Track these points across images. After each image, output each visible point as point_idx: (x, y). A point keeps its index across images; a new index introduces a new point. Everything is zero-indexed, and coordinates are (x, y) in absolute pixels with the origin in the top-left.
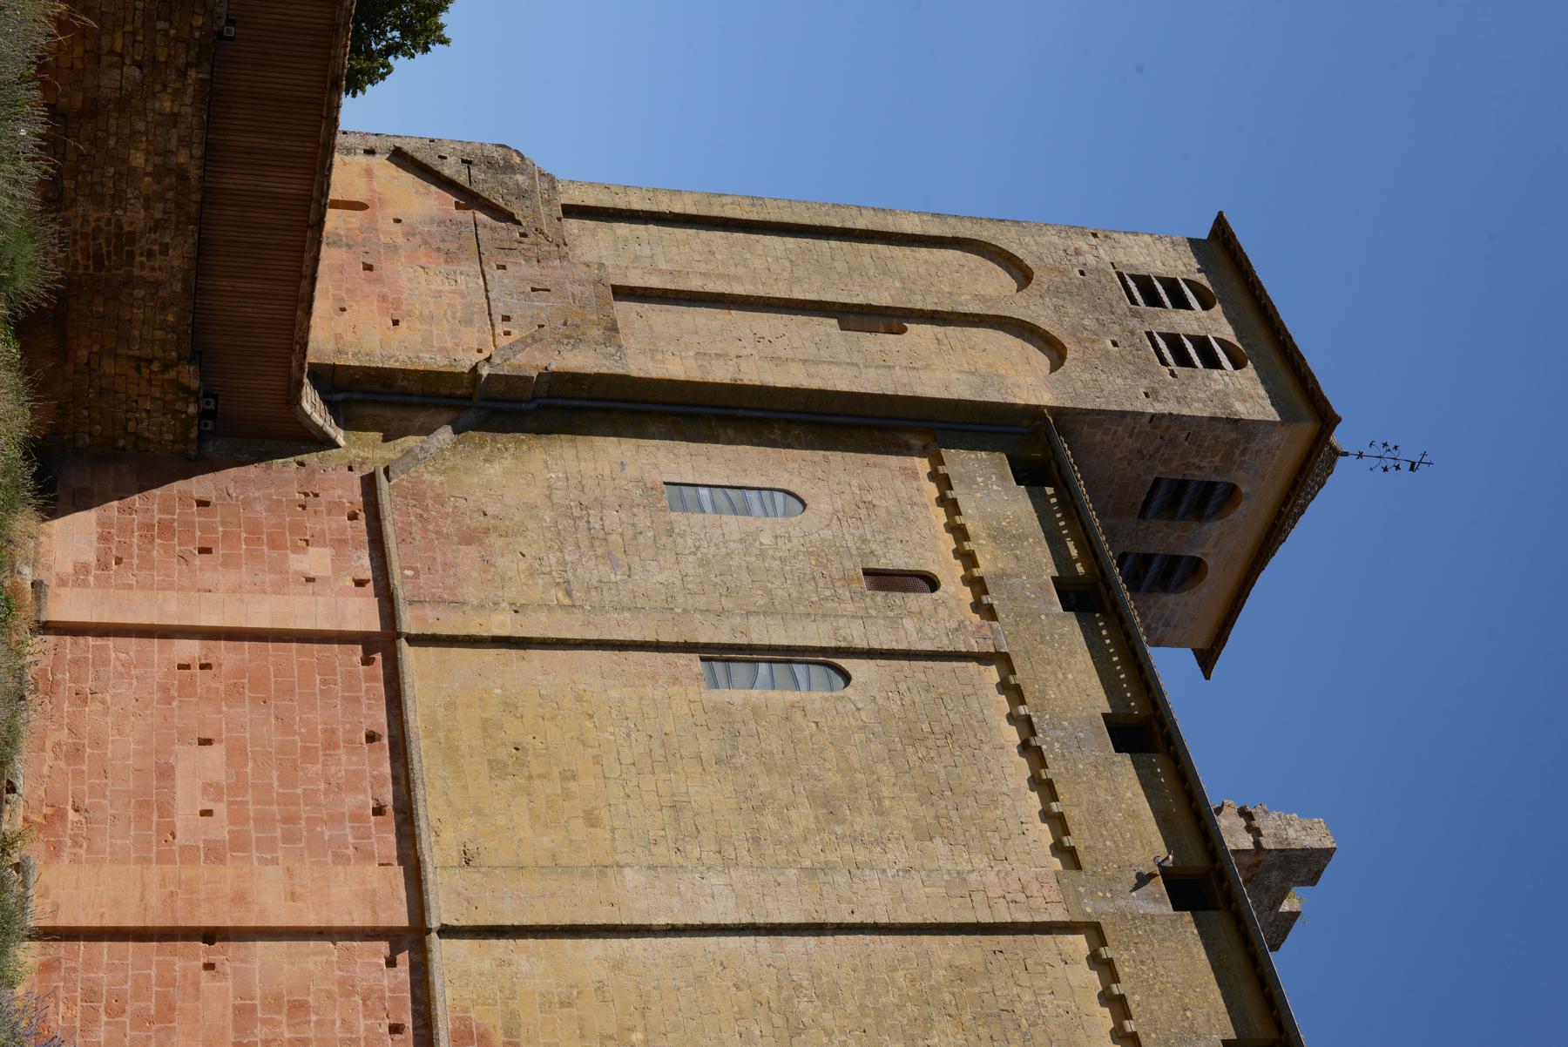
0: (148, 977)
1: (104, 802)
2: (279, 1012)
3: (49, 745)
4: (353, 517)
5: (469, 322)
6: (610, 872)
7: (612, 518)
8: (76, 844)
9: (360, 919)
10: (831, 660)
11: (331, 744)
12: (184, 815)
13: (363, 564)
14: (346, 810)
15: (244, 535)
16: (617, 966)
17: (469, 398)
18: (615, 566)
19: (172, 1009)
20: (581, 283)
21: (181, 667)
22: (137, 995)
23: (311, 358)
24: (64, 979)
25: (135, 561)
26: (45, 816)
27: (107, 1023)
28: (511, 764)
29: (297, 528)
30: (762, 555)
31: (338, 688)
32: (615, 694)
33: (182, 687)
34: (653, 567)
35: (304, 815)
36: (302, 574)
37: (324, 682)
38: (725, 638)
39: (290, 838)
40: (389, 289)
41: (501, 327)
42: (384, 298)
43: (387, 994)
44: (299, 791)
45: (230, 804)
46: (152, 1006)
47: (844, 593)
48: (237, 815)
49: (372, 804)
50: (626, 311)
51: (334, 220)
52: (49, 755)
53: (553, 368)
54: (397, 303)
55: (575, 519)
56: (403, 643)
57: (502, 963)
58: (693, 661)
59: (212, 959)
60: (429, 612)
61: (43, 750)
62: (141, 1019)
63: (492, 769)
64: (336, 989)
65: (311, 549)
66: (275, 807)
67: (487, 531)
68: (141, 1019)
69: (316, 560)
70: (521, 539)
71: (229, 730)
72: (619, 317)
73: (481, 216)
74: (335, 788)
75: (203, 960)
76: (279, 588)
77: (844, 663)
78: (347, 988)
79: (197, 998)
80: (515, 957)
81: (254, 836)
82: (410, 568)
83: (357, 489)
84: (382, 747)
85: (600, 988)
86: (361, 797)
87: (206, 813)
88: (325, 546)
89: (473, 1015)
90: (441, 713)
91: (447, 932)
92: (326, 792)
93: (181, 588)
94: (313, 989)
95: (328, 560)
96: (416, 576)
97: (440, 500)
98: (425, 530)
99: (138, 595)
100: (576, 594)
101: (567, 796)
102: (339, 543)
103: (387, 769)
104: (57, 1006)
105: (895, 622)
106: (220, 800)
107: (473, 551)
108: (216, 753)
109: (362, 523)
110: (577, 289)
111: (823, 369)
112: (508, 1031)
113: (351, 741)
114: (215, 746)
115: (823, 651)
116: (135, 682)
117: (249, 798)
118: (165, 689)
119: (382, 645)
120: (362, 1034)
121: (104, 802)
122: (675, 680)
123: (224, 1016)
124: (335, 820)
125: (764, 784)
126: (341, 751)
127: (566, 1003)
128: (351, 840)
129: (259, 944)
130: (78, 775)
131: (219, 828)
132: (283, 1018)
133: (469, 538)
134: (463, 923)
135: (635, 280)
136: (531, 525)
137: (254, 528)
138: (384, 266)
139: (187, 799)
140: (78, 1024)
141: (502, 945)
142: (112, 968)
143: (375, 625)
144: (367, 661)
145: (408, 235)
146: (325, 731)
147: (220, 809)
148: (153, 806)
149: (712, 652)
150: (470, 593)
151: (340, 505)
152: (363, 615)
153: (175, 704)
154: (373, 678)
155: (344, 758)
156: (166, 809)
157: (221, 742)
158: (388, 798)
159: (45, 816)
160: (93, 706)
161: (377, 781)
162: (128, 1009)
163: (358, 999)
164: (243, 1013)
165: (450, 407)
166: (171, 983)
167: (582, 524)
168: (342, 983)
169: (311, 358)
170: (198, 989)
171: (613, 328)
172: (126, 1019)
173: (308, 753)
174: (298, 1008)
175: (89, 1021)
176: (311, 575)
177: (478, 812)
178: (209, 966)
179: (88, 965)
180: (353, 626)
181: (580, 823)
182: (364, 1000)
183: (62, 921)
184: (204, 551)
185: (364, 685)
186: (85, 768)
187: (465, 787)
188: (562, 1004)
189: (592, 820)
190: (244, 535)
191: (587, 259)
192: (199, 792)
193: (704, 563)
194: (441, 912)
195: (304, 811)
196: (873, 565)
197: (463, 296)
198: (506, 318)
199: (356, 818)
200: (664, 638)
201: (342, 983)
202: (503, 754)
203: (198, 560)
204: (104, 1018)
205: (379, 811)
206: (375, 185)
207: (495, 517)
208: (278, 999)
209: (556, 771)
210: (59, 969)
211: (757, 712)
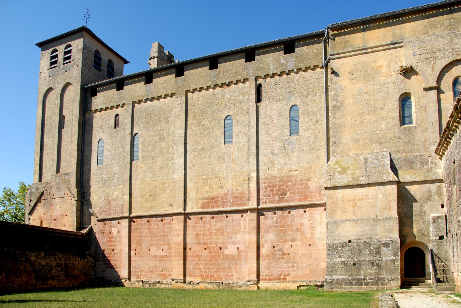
4: (106, 224)
5: (66, 202)
6: (174, 180)
7: (105, 176)
9: (182, 224)
10: (133, 136)
11: (150, 229)
12: (163, 253)
13: (115, 222)
16: (191, 180)
17: (81, 202)
18: (114, 176)
20: (56, 179)
22: (195, 261)
23: (75, 231)
28: (153, 197)
29: (108, 234)
30: (111, 148)
32: (140, 178)
33: (139, 254)
34: (114, 169)
38: (129, 156)
39: (167, 236)
40: (60, 215)
41: (66, 195)
42: (61, 217)
47: (119, 133)
48: (163, 245)
50: (62, 171)
51: (44, 225)
53: (75, 186)
54: (62, 215)
56: (131, 216)
57: (190, 200)
58: (134, 162)
60: (124, 211)
67: (108, 200)
69: (114, 231)
72: (63, 173)
73: (43, 198)
74: (158, 228)
76: (120, 237)
77: (134, 134)
78: (194, 226)
83: (100, 223)
85: (195, 183)
87: (163, 250)
90: (144, 209)
91: (185, 209)
93: (121, 254)
97: (102, 208)
98: (108, 211)
99: (123, 262)
100: (120, 184)
101: (159, 187)
102: (111, 227)
103: (154, 219)
105: (126, 124)
107: (112, 202)
109: (107, 222)
110: (57, 180)
111: (73, 133)
112: (202, 199)
113: (149, 225)
115: (131, 138)
117: (160, 243)
118: (140, 257)
119: (131, 219)
122: (137, 166)
124: (164, 228)
125: (157, 151)
127: (198, 189)
129: (187, 241)
131: (166, 248)
133: (109, 203)
134: (183, 206)
135: (55, 168)
136: (106, 191)
137: (109, 242)
138: (55, 218)
139: (160, 253)
141: (188, 200)
142: (190, 265)
143: (127, 220)
144: (134, 222)
145: (47, 212)
147: (162, 248)
149: (132, 159)
150: (120, 203)
151: (103, 226)
152: (125, 223)
154: (137, 221)
158: (160, 219)
161: (157, 221)
165: (83, 206)
167: (106, 182)
168: (193, 227)
169: (75, 231)
171: (66, 174)
173: (151, 233)
174: (198, 235)
177: (162, 203)
179: (190, 269)
180: (127, 224)
181: (165, 185)
183: (182, 273)
184: (113, 250)
188: (198, 190)
189: (164, 183)
191: (50, 178)
193: (113, 159)
194: (181, 210)
195: (162, 233)
196: (114, 126)
197: (60, 202)
198: (65, 194)
199: (163, 224)
200: (129, 168)
201: (193, 227)
202: (151, 198)
203: (115, 251)
205: (162, 220)
206: (37, 218)
208: (196, 238)
209: (155, 189)
211: (143, 151)
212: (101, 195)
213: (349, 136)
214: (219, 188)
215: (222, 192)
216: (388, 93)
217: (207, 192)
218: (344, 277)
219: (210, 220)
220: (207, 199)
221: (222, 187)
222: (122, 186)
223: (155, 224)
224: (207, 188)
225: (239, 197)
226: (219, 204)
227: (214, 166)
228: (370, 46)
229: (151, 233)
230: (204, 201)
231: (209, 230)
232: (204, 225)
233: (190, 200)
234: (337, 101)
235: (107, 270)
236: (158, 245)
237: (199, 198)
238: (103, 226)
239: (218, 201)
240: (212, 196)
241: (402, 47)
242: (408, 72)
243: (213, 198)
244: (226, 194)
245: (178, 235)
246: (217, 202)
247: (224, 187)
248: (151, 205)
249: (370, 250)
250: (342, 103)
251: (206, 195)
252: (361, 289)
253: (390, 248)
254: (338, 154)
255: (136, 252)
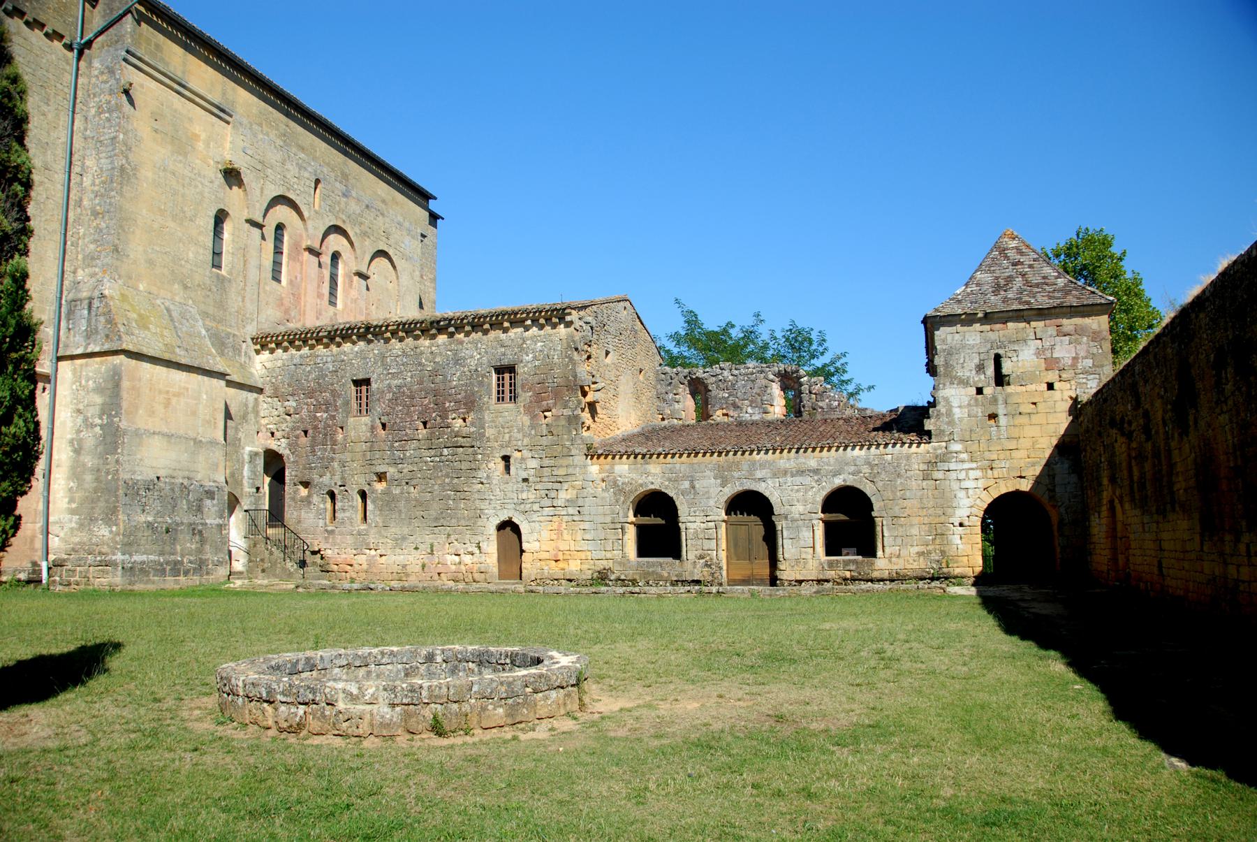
213: (140, 249)
216: (201, 193)
218: (152, 557)
228: (190, 85)
234: (127, 158)
241: (228, 123)
242: (232, 176)
249: (188, 501)
250: (135, 169)
252: (177, 582)
253: (215, 502)
254: (120, 277)
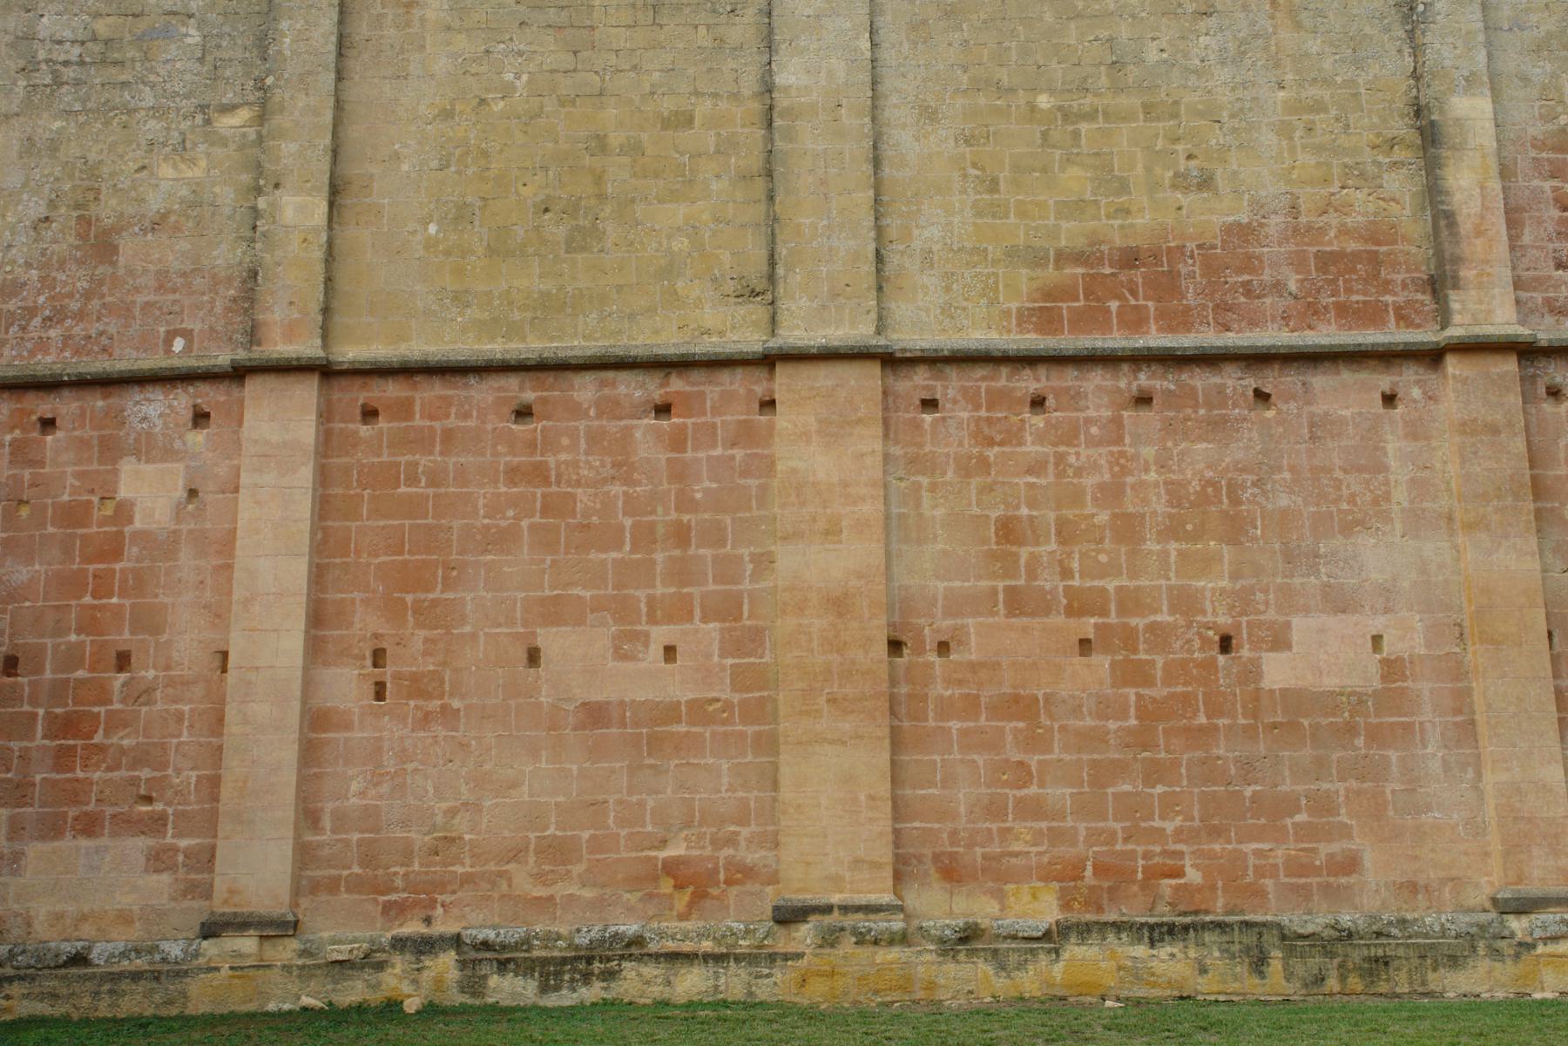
0: (964, 733)
1: (650, 803)
2: (1016, 556)
3: (541, 892)
8: (732, 841)
11: (539, 474)
12: (677, 687)
14: (663, 457)
15: (88, 599)
19: (1016, 699)
21: (380, 694)
24: (971, 845)
25: (145, 773)
26: (679, 887)
27: (1042, 785)
31: (424, 461)
35: (673, 516)
36: (179, 513)
37: (413, 480)
43: (983, 413)
44: (628, 522)
45: (653, 620)
46: (1010, 726)
48: (679, 611)
49: (650, 421)
52: (561, 890)
55: (58, 82)
59: (930, 643)
61: (551, 898)
62: (1035, 741)
63: (583, 249)
64: (975, 482)
65: (123, 493)
66: (659, 557)
67: (86, 222)
68: (1035, 741)
70: (105, 170)
71: (511, 622)
74: (624, 470)
75: (933, 657)
79: (996, 666)
80: (917, 244)
81: (712, 587)
82: (168, 343)
84: (544, 401)
86: (638, 435)
87: (670, 652)
88: (115, 472)
89: (1014, 305)
90: (474, 313)
92: (628, 481)
94: (976, 510)
95: (144, 467)
96: (187, 334)
98: (80, 316)
102: (111, 450)
104: (1016, 855)
106: (647, 635)
107: (128, 247)
108: (551, 640)
112: (1037, 259)
113: (532, 446)
114: (540, 642)
116: (410, 767)
117: (641, 594)
118: (426, 719)
120: (1048, 449)
121: (650, 803)
123: (1024, 629)
124: (680, 473)
126: (551, 460)
128: (718, 451)
130: (596, 844)
132: (1024, 553)
133: (100, 245)
137: (71, 584)
139: (644, 681)
140: (1044, 825)
146: (511, 482)
148: (655, 732)
153: (456, 704)
155: (563, 457)
156: (670, 712)
157: (534, 634)
159: (679, 887)
160: (461, 824)
161: (609, 408)
162: (1016, 757)
163: (992, 453)
164: (1017, 603)
166: (971, 706)
167: (69, 73)
170: (982, 665)
172: (1034, 760)
175: (1032, 809)
176: (181, 493)
178: (943, 648)
182: (991, 443)
184: (123, 661)
185: (418, 422)
186: (586, 835)
187: (619, 288)
188: (993, 186)
190: (88, 599)
192: (629, 666)
195: (665, 516)
199: (677, 442)
204: (1033, 790)
207: (52, 205)
210: (953, 856)
212: (14, 180)
214: (1181, 182)
215: (1208, 216)
217: (1076, 208)
219: (1117, 422)
220: (1079, 258)
221: (1206, 183)
222: (244, 114)
223: (594, 438)
224: (1076, 180)
225: (1356, 255)
226: (1191, 299)
227: (1124, 32)
229: (546, 510)
230: (1050, 274)
231: (1111, 493)
232: (1060, 459)
233: (928, 259)
235: (35, 850)
236: (622, 609)
237: (1012, 254)
238: (18, 448)
239: (1173, 275)
240: (1118, 242)
243: (1130, 258)
244: (1242, 233)
245: (832, 532)
246: (1166, 286)
247: (1220, 181)
248: (548, 285)
251: (1071, 233)
255: (387, 673)
